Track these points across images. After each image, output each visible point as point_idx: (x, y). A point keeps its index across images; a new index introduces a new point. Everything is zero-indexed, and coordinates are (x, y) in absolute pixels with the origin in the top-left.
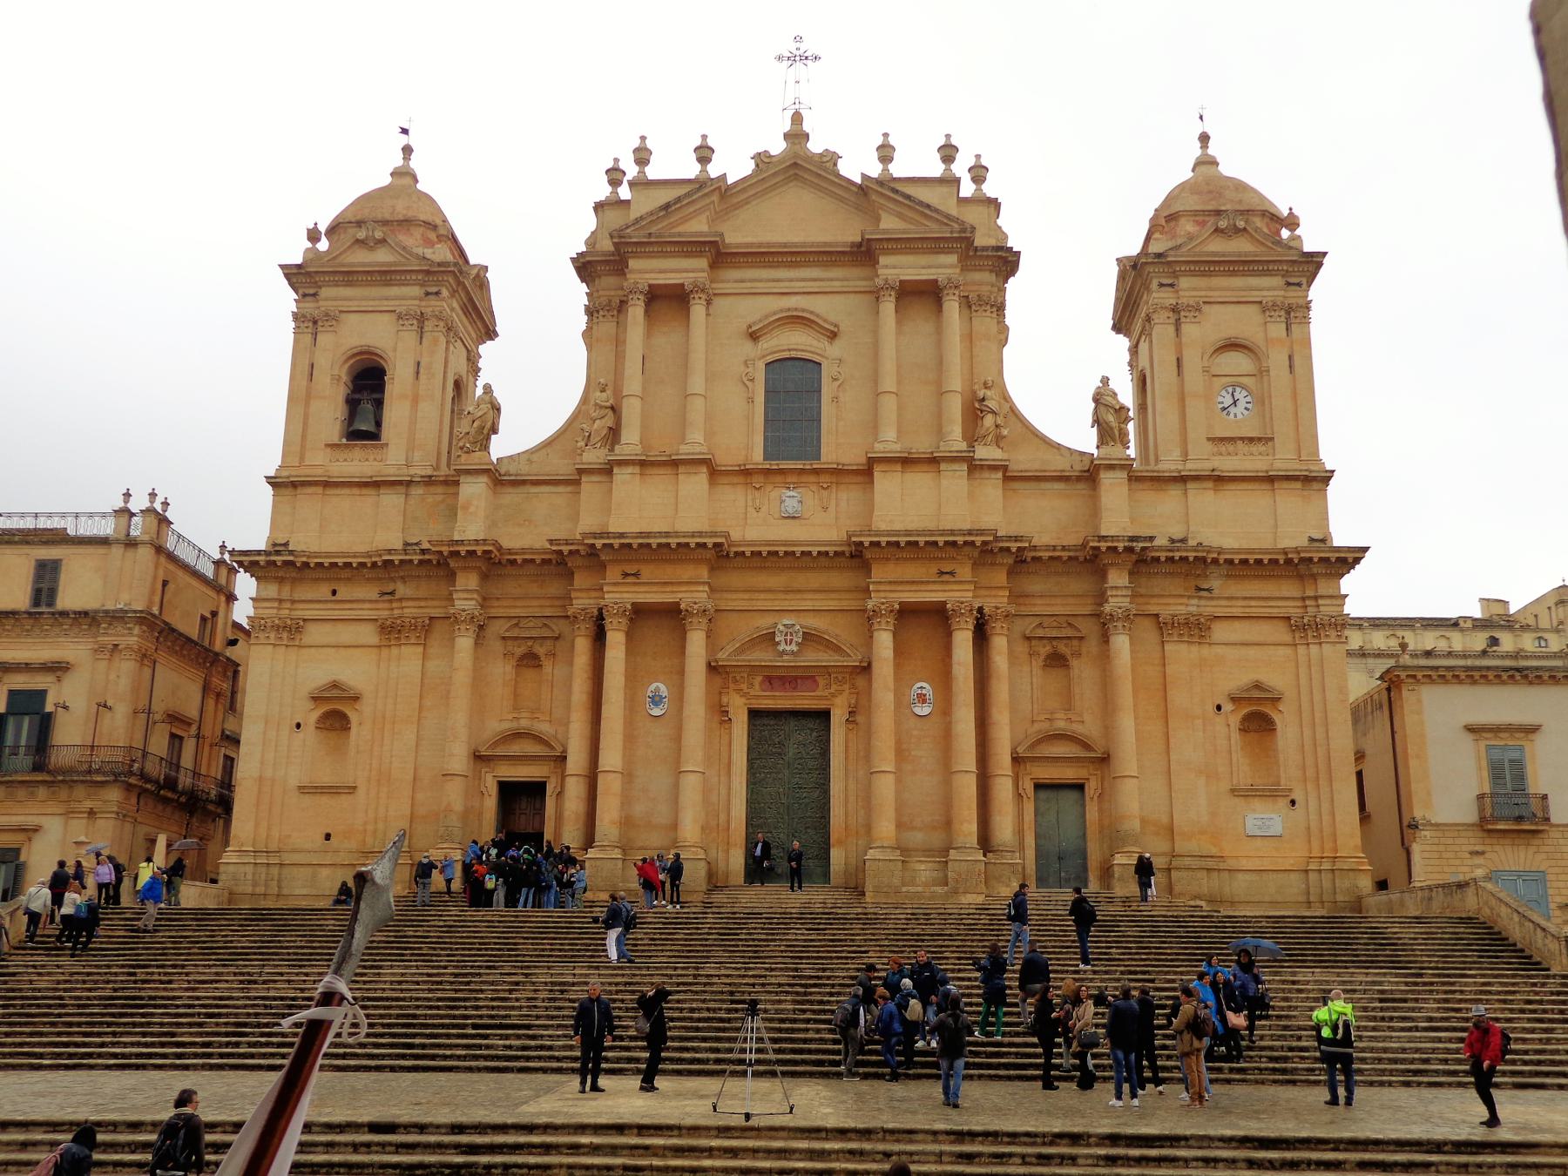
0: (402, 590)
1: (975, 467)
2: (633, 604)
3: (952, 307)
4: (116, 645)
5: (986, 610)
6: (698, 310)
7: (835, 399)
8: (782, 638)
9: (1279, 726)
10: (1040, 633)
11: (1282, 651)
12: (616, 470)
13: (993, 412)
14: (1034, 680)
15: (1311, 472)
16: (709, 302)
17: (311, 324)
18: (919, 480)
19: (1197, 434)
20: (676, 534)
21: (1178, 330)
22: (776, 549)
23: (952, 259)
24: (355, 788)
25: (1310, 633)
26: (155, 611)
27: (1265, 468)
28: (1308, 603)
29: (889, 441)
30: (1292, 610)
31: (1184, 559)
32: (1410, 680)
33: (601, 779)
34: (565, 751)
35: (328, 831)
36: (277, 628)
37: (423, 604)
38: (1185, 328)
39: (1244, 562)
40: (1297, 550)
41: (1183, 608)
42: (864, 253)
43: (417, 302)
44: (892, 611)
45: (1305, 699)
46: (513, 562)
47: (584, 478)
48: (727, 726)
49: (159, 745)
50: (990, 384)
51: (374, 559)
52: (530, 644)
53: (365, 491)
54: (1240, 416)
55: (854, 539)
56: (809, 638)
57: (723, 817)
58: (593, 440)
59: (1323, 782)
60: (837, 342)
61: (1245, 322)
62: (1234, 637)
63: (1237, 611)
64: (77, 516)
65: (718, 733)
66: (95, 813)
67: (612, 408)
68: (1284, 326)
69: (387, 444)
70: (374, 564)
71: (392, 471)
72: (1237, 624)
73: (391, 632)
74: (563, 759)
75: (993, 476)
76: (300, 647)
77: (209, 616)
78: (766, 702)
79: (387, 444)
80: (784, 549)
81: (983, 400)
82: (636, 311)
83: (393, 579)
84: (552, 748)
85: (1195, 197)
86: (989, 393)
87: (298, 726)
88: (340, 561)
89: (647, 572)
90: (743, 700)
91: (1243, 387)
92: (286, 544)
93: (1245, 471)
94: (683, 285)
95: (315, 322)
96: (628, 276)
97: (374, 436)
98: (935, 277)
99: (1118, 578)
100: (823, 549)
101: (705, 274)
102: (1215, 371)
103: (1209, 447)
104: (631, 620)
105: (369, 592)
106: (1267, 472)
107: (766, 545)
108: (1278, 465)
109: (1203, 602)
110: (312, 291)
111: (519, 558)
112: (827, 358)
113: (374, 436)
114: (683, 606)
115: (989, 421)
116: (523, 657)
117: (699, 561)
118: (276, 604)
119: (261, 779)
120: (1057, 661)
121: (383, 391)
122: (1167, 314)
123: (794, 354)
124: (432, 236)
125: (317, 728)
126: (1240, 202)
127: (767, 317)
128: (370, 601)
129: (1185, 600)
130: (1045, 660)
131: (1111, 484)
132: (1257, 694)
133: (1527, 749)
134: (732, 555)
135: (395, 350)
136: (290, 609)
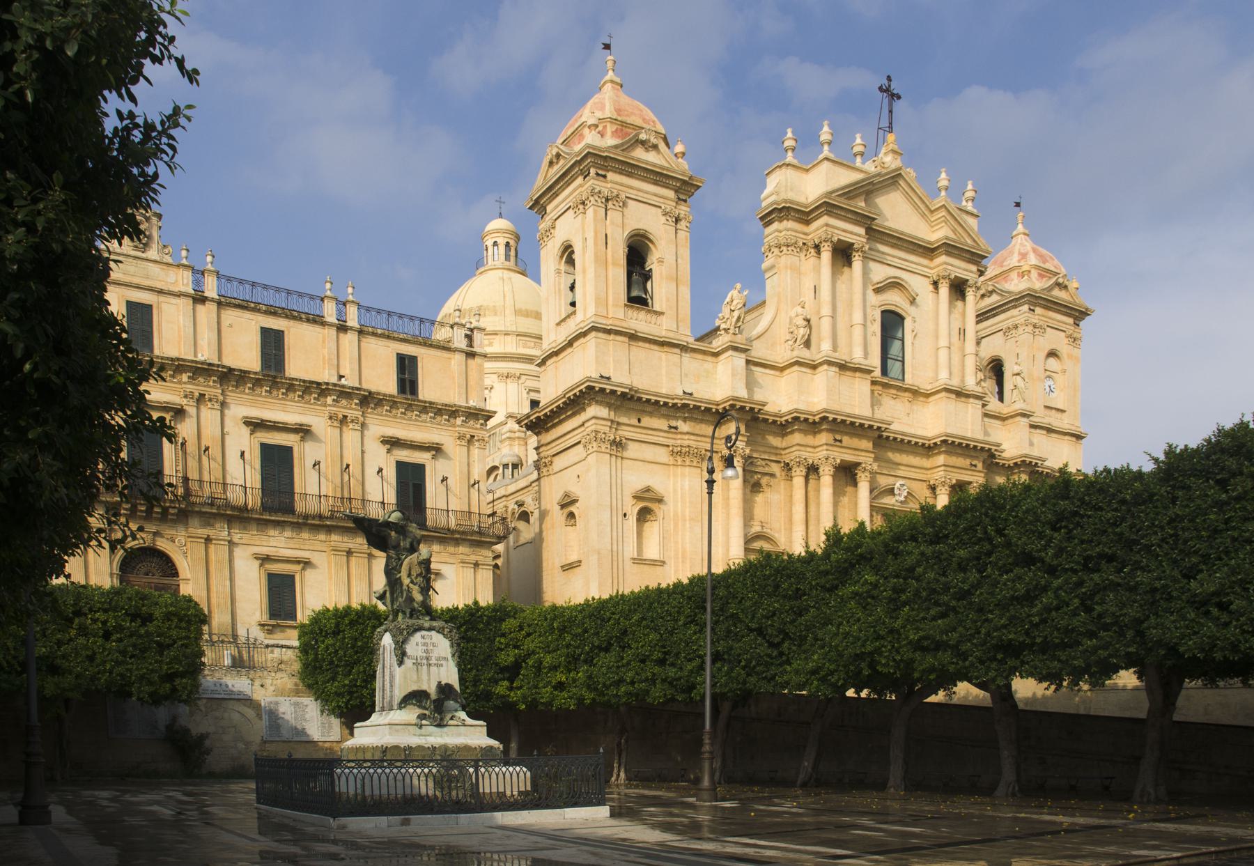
0: (684, 426)
37: (699, 439)
51: (675, 401)
53: (653, 347)
83: (677, 418)
87: (625, 515)
89: (846, 440)
105: (662, 424)
117: (868, 438)
128: (665, 431)
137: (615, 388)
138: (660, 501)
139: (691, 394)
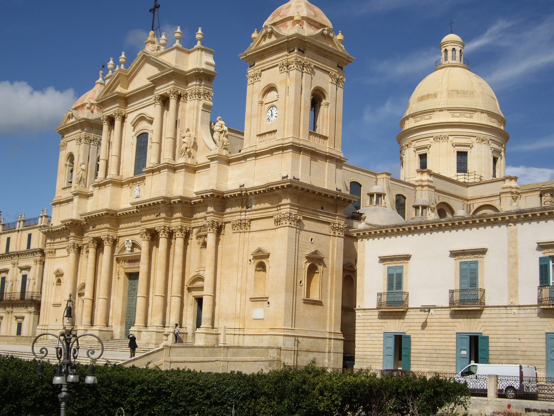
11: (272, 232)
24: (61, 304)
54: (273, 121)
62: (258, 228)
63: (258, 216)
72: (260, 221)
76: (54, 258)
93: (272, 147)
129: (239, 214)
133: (404, 267)
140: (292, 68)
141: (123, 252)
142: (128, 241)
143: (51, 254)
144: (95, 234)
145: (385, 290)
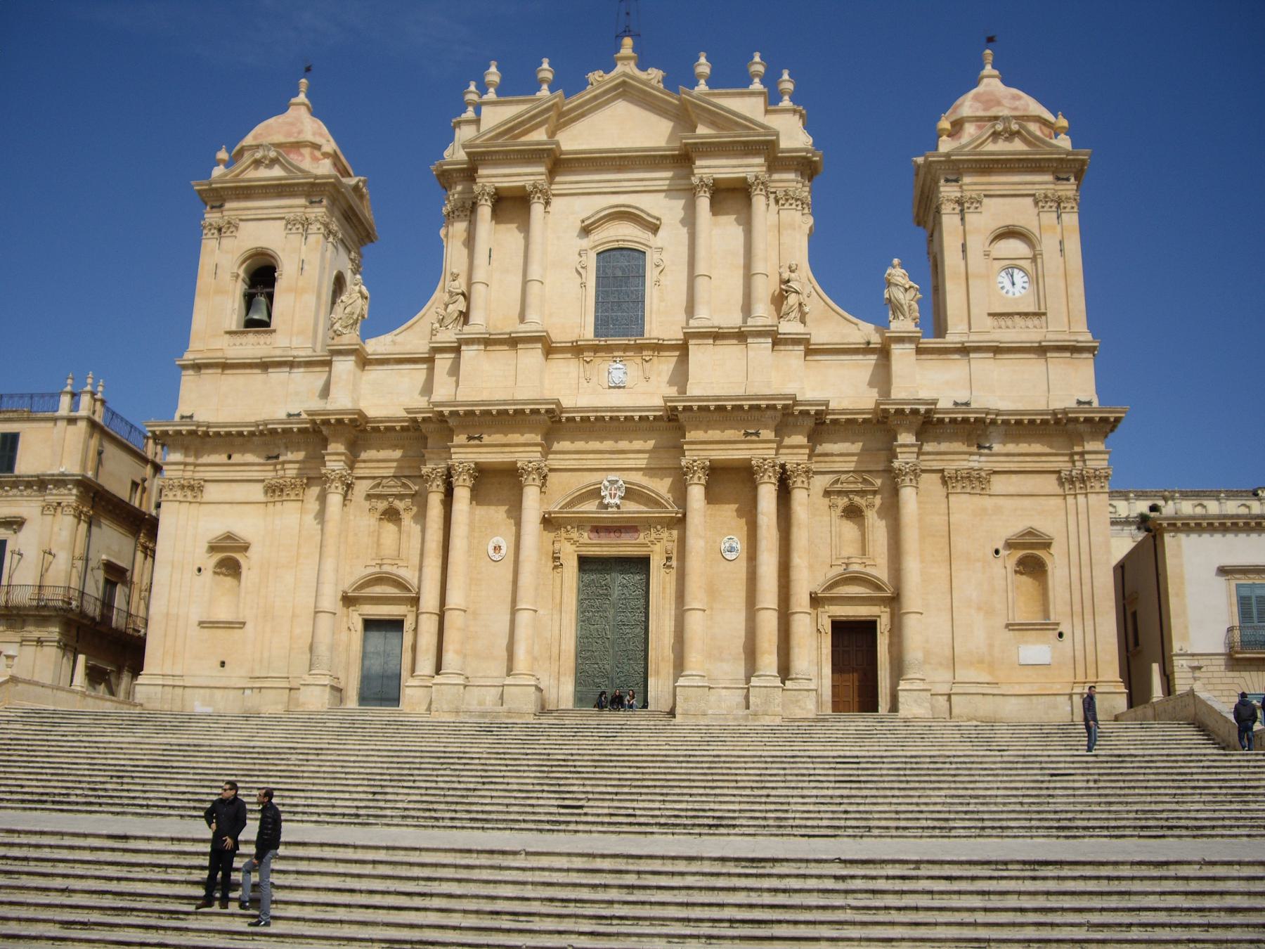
1: (778, 341)
2: (476, 464)
3: (759, 201)
4: (59, 504)
5: (788, 467)
6: (537, 208)
7: (657, 283)
8: (607, 493)
9: (1050, 568)
10: (838, 487)
12: (463, 348)
13: (797, 292)
14: (833, 529)
15: (1078, 342)
16: (547, 203)
17: (216, 231)
18: (729, 352)
19: (979, 311)
20: (515, 402)
21: (962, 219)
22: (603, 414)
23: (760, 160)
24: (244, 623)
25: (1078, 485)
26: (90, 474)
27: (1039, 340)
28: (1076, 457)
29: (707, 317)
30: (1061, 465)
31: (965, 420)
32: (1171, 528)
33: (448, 616)
34: (418, 593)
35: (222, 659)
36: (182, 487)
38: (968, 217)
39: (1019, 422)
40: (1065, 412)
41: (965, 463)
42: (683, 159)
43: (303, 209)
44: (703, 468)
45: (1073, 542)
46: (376, 429)
47: (437, 356)
48: (559, 570)
49: (95, 586)
50: (794, 267)
51: (261, 428)
52: (391, 500)
55: (669, 404)
56: (631, 493)
57: (555, 651)
58: (447, 321)
59: (1088, 617)
60: (660, 233)
61: (1021, 213)
62: (1012, 490)
63: (1013, 467)
64: (32, 396)
65: (551, 577)
66: (42, 642)
67: (463, 294)
68: (1054, 215)
69: (274, 331)
70: (261, 433)
71: (278, 352)
73: (275, 490)
74: (418, 599)
75: (796, 348)
76: (200, 503)
77: (139, 481)
78: (593, 549)
79: (274, 331)
80: (609, 414)
81: (788, 281)
82: (485, 211)
84: (410, 590)
85: (977, 105)
86: (793, 275)
87: (200, 570)
88: (234, 430)
90: (574, 547)
91: (1021, 269)
92: (191, 417)
94: (524, 187)
95: (220, 230)
96: (478, 180)
97: (264, 324)
98: (744, 175)
99: (906, 438)
100: (644, 414)
101: (544, 177)
102: (995, 254)
103: (990, 321)
104: (476, 478)
106: (1040, 342)
107: (593, 411)
108: (1050, 336)
109: (983, 459)
110: (218, 204)
111: (382, 426)
112: (650, 247)
113: (264, 324)
114: (519, 465)
115: (792, 299)
116: (385, 513)
118: (182, 467)
119: (168, 614)
120: (853, 513)
121: (273, 286)
122: (952, 206)
123: (621, 245)
124: (318, 154)
125: (215, 573)
126: (1015, 109)
127: (598, 212)
130: (843, 511)
131: (901, 354)
132: (1029, 540)
134: (564, 420)
135: (284, 250)
136: (193, 471)
137: (178, 428)
138: (245, 548)
139: (299, 415)
140: (1067, 210)
141: (574, 506)
142: (612, 482)
143: (189, 493)
144: (482, 456)
145: (1236, 623)
